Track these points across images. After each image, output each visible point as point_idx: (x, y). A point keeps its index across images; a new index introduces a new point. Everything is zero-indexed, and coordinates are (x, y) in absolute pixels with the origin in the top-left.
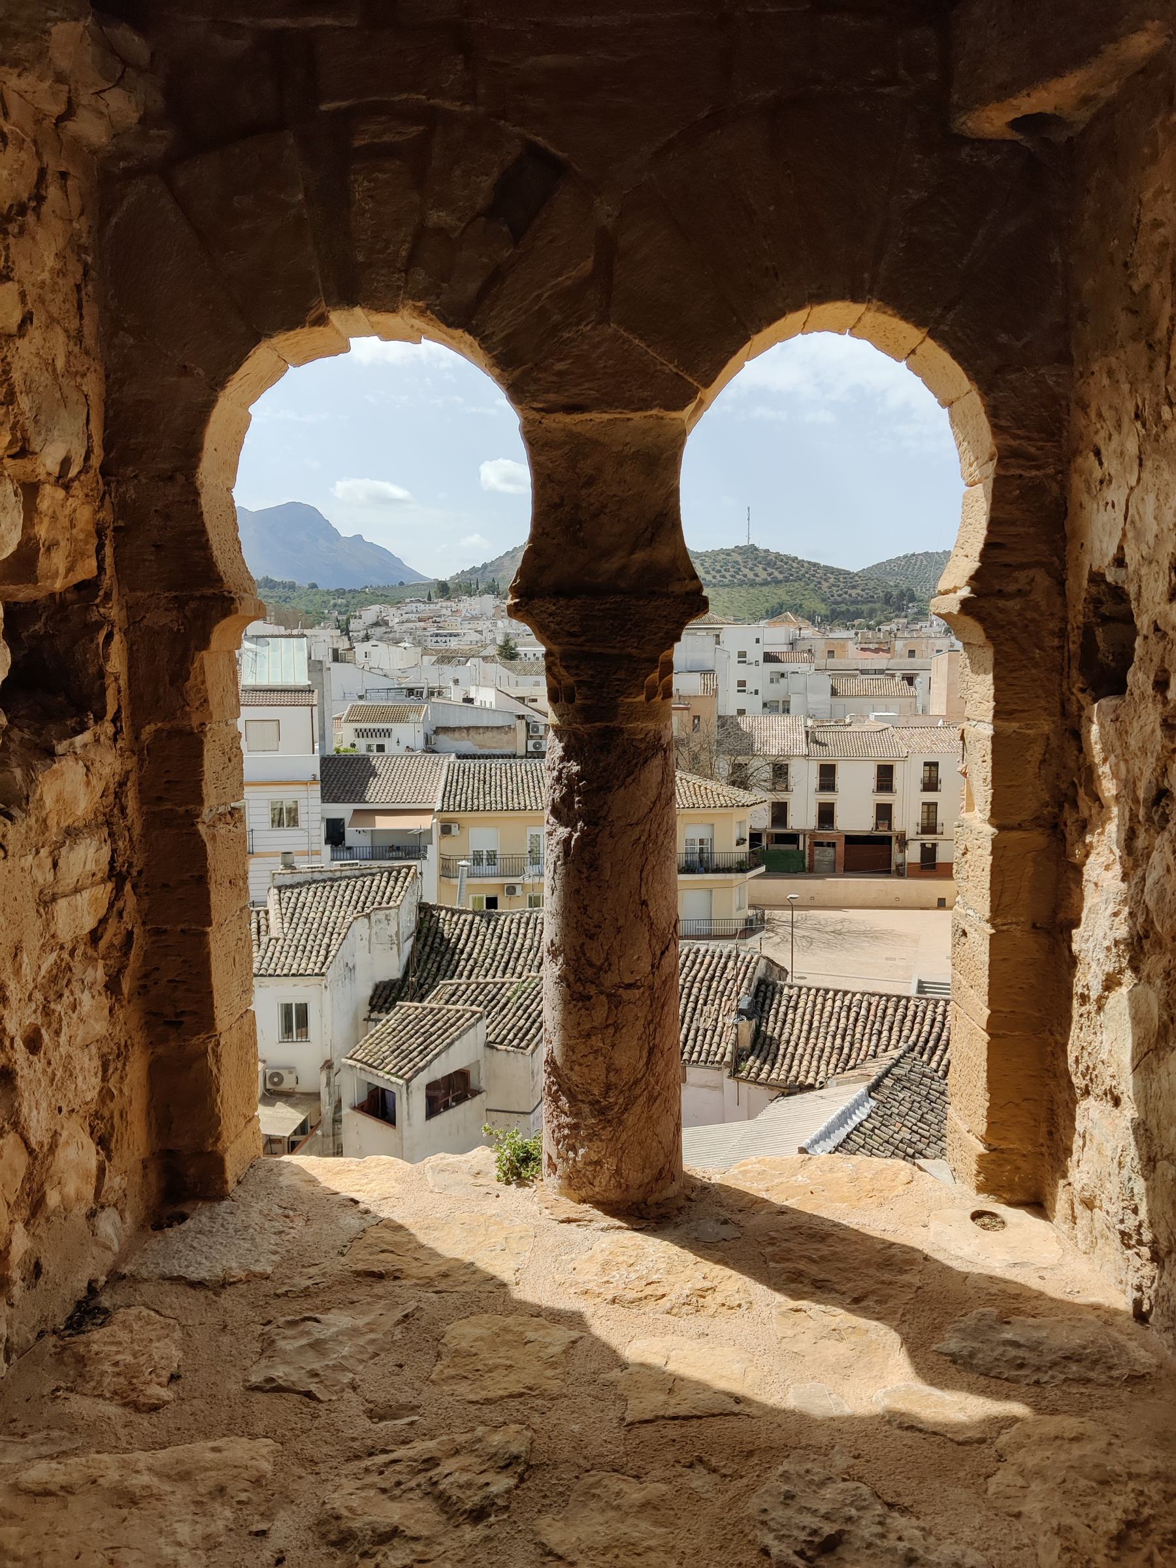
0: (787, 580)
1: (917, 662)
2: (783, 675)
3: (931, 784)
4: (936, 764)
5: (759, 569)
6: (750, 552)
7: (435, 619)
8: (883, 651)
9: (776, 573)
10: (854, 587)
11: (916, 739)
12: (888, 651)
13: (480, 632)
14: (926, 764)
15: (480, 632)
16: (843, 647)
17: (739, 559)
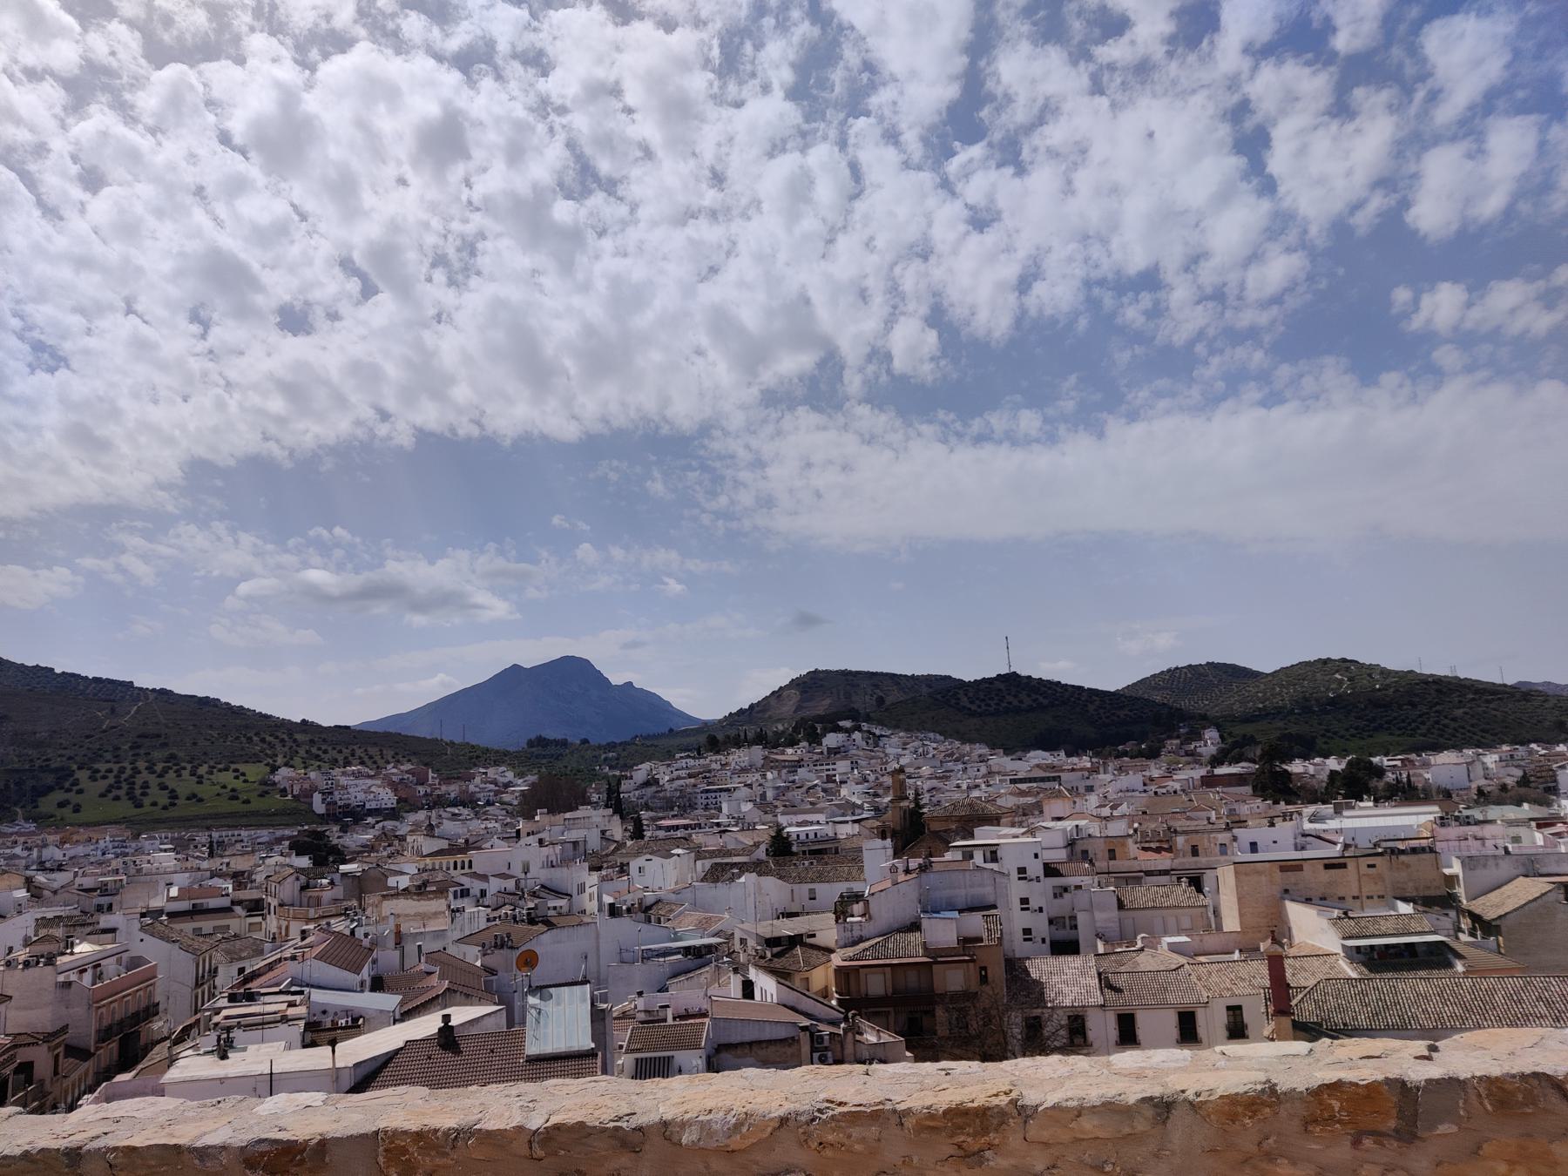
1: (1202, 860)
2: (1066, 889)
4: (1239, 1008)
5: (1023, 696)
6: (1011, 679)
7: (706, 774)
9: (1041, 699)
10: (1122, 708)
11: (1214, 978)
12: (1169, 850)
13: (750, 786)
14: (1229, 1008)
15: (750, 786)
16: (1124, 845)
17: (1002, 686)
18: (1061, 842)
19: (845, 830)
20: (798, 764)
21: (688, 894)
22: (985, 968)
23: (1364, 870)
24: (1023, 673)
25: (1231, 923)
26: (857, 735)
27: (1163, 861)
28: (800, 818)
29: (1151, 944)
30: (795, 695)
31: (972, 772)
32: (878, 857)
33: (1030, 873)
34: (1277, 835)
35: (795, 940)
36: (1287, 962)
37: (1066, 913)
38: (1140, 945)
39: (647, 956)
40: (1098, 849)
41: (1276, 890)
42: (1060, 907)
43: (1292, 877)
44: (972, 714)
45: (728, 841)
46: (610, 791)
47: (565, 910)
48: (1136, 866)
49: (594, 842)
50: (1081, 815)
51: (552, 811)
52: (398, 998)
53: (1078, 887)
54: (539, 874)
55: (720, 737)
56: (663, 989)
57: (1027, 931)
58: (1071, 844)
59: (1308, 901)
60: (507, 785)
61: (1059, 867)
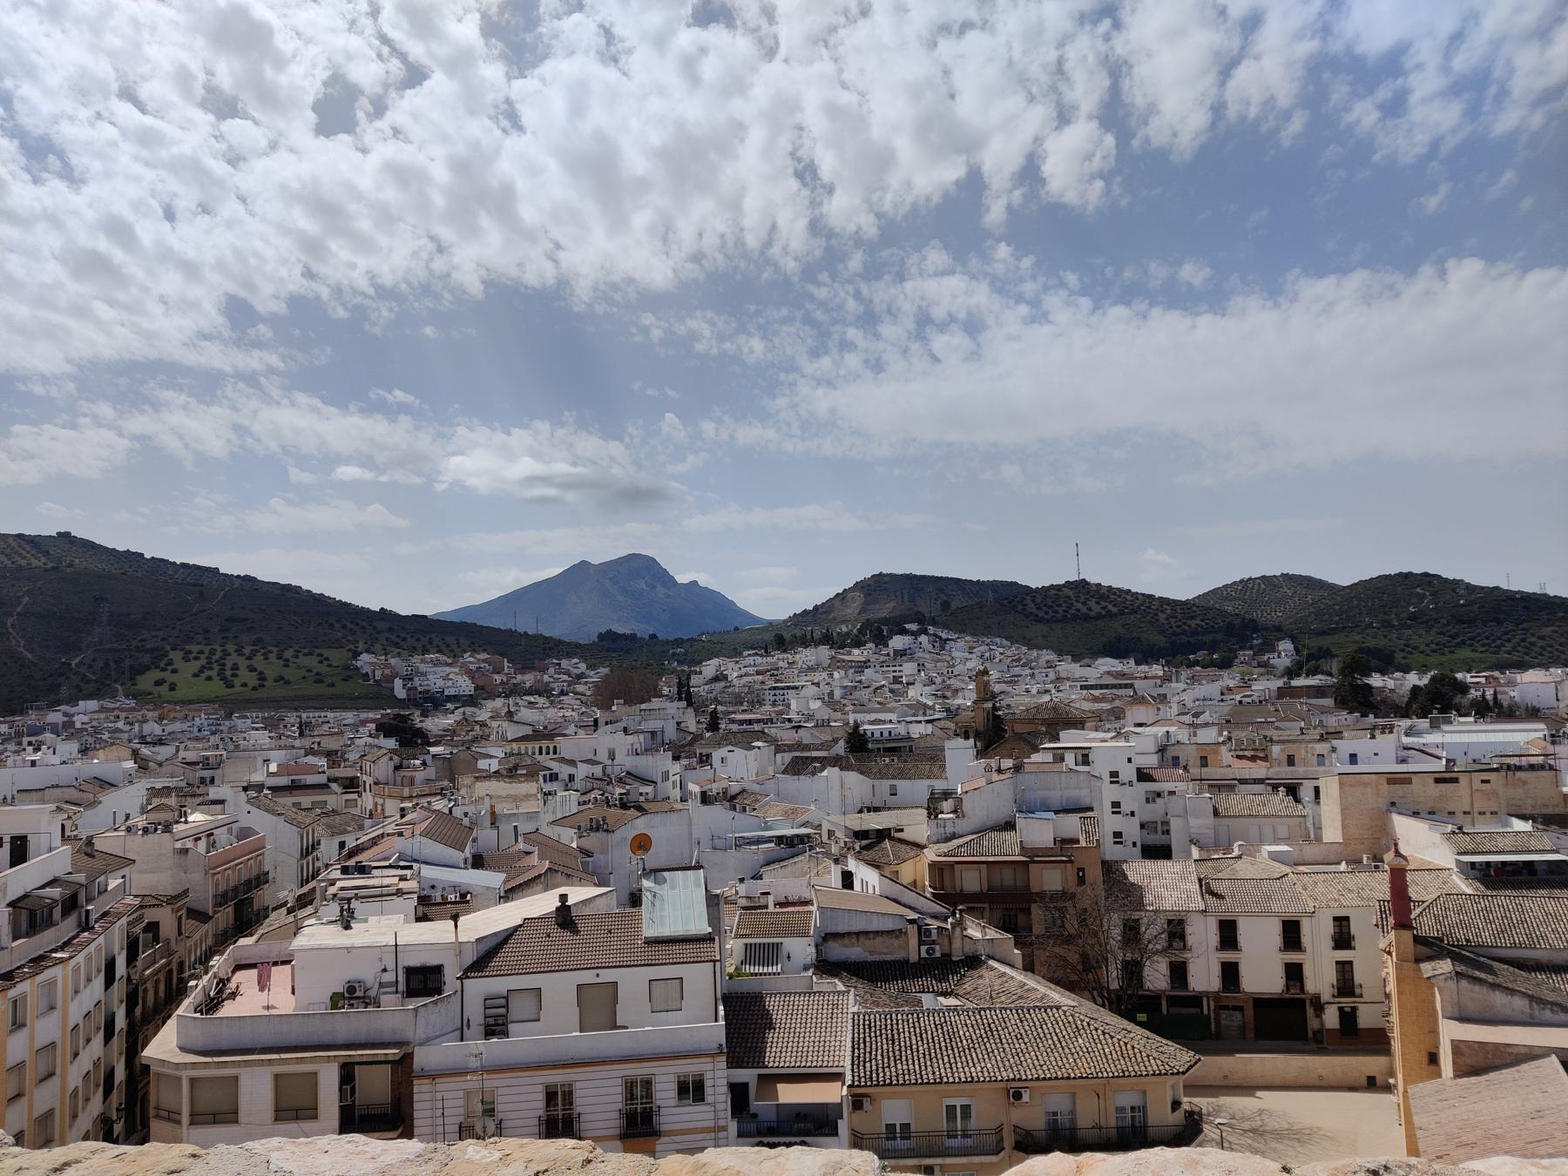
0: (1122, 613)
1: (1299, 770)
2: (1159, 795)
3: (1343, 939)
4: (1347, 919)
5: (1092, 603)
6: (1081, 586)
7: (774, 672)
8: (1261, 759)
9: (1110, 607)
10: (1192, 618)
11: (1321, 888)
12: (1265, 759)
14: (1335, 919)
15: (817, 685)
16: (1216, 752)
18: (1153, 748)
19: (917, 730)
20: (863, 666)
21: (770, 785)
22: (1082, 870)
23: (1477, 784)
24: (1093, 579)
25: (1332, 833)
26: (923, 638)
27: (1258, 770)
28: (873, 716)
29: (1250, 850)
30: (859, 598)
31: (1039, 677)
32: (961, 757)
33: (1122, 778)
34: (1379, 749)
35: (883, 834)
36: (1409, 877)
37: (1159, 817)
38: (1236, 853)
39: (740, 843)
40: (1189, 755)
41: (1382, 803)
42: (1153, 812)
43: (1399, 790)
44: (1039, 620)
45: (805, 736)
46: (680, 685)
47: (650, 797)
48: (1229, 773)
49: (671, 733)
50: (1168, 721)
51: (630, 701)
52: (503, 876)
53: (1172, 793)
54: (625, 761)
55: (787, 636)
56: (757, 877)
57: (1118, 835)
58: (1162, 750)
59: (1416, 814)
60: (580, 676)
61: (1152, 772)
